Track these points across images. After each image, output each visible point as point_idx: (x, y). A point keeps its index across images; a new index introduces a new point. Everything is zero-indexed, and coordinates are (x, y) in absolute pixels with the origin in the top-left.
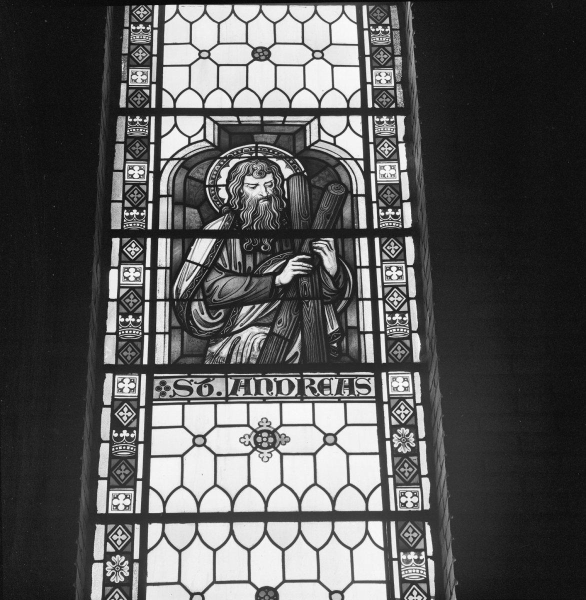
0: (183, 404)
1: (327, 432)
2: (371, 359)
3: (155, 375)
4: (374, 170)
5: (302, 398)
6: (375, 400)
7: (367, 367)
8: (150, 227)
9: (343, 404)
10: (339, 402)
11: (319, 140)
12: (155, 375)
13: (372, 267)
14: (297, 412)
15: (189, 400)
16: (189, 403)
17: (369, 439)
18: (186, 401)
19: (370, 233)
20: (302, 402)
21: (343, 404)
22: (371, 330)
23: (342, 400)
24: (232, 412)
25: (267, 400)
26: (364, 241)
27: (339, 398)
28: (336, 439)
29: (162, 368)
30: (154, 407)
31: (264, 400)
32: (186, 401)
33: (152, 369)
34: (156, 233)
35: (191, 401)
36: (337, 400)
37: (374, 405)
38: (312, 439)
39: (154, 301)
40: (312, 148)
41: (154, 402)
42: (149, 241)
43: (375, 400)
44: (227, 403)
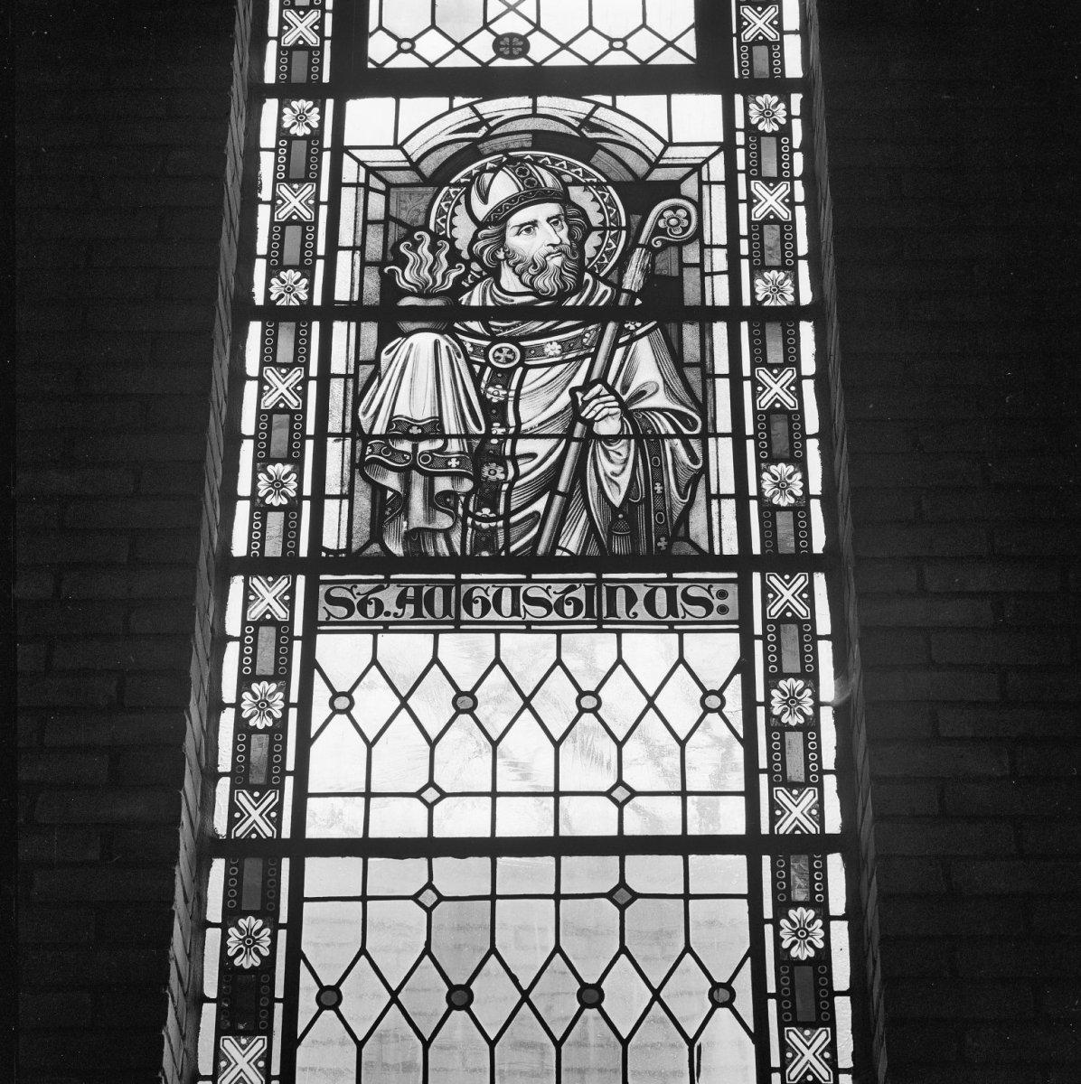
0: (375, 633)
2: (731, 547)
3: (323, 577)
6: (736, 627)
7: (723, 563)
8: (317, 301)
9: (675, 637)
10: (671, 631)
12: (323, 577)
13: (735, 377)
16: (386, 631)
19: (733, 314)
20: (600, 630)
21: (675, 637)
26: (720, 330)
27: (671, 624)
30: (320, 637)
34: (331, 311)
35: (390, 627)
36: (666, 627)
37: (737, 636)
39: (322, 435)
42: (316, 326)
43: (736, 627)
44: (457, 630)
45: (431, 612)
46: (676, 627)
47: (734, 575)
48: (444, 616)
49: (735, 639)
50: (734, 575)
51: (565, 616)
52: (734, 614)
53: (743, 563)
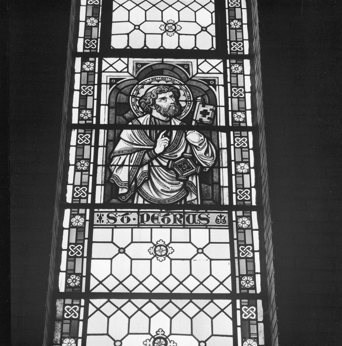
0: (113, 228)
1: (198, 247)
4: (229, 39)
5: (184, 227)
6: (228, 227)
7: (224, 207)
9: (208, 230)
10: (206, 228)
11: (198, 73)
14: (180, 234)
15: (116, 225)
16: (116, 228)
17: (225, 251)
18: (114, 227)
20: (184, 228)
21: (208, 230)
22: (227, 185)
23: (208, 227)
24: (142, 234)
25: (163, 226)
28: (203, 251)
29: (99, 206)
30: (94, 230)
31: (161, 227)
32: (114, 227)
33: (93, 206)
35: (117, 226)
38: (189, 251)
40: (193, 78)
41: (94, 226)
43: (228, 227)
44: (138, 228)
45: (189, 222)
46: (208, 227)
47: (227, 211)
48: (193, 223)
49: (227, 231)
50: (227, 211)
51: (190, 224)
52: (227, 224)
53: (230, 208)
